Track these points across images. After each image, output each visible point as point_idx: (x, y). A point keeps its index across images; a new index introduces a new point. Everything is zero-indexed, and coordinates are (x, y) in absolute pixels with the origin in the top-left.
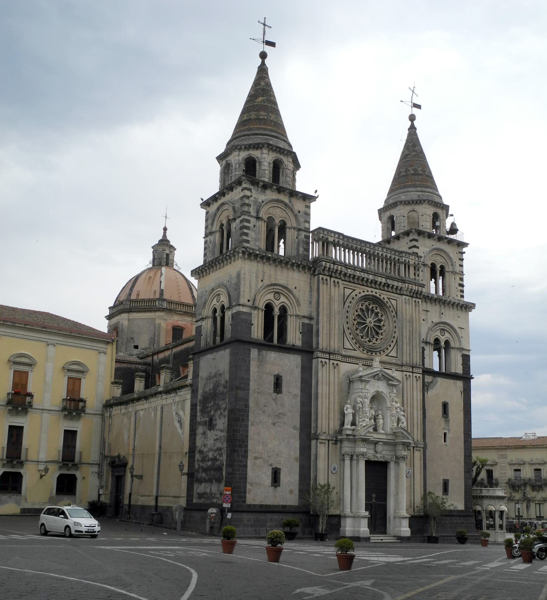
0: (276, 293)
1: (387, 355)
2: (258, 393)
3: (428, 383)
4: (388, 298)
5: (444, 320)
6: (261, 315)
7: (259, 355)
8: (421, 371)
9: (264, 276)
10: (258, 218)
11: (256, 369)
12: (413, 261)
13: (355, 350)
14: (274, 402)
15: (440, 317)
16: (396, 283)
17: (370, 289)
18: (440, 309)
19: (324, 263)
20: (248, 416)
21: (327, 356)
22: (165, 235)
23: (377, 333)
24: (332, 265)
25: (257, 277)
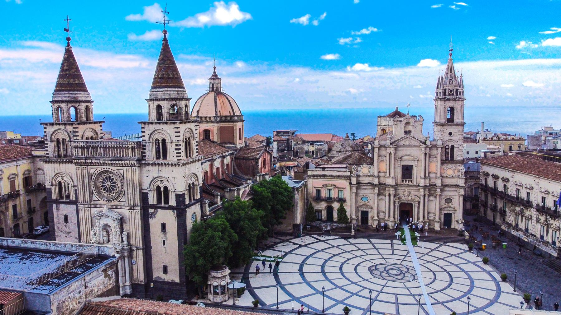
0: (62, 176)
1: (119, 201)
2: (58, 223)
3: (151, 213)
4: (118, 170)
5: (160, 175)
6: (57, 188)
7: (56, 206)
8: (139, 208)
9: (55, 170)
10: (51, 141)
11: (56, 213)
12: (131, 145)
13: (99, 200)
14: (65, 227)
15: (158, 173)
16: (117, 162)
17: (105, 167)
18: (159, 168)
19: (73, 160)
20: (55, 233)
21: (83, 206)
22: (215, 72)
23: (114, 190)
24: (78, 161)
25: (52, 171)
